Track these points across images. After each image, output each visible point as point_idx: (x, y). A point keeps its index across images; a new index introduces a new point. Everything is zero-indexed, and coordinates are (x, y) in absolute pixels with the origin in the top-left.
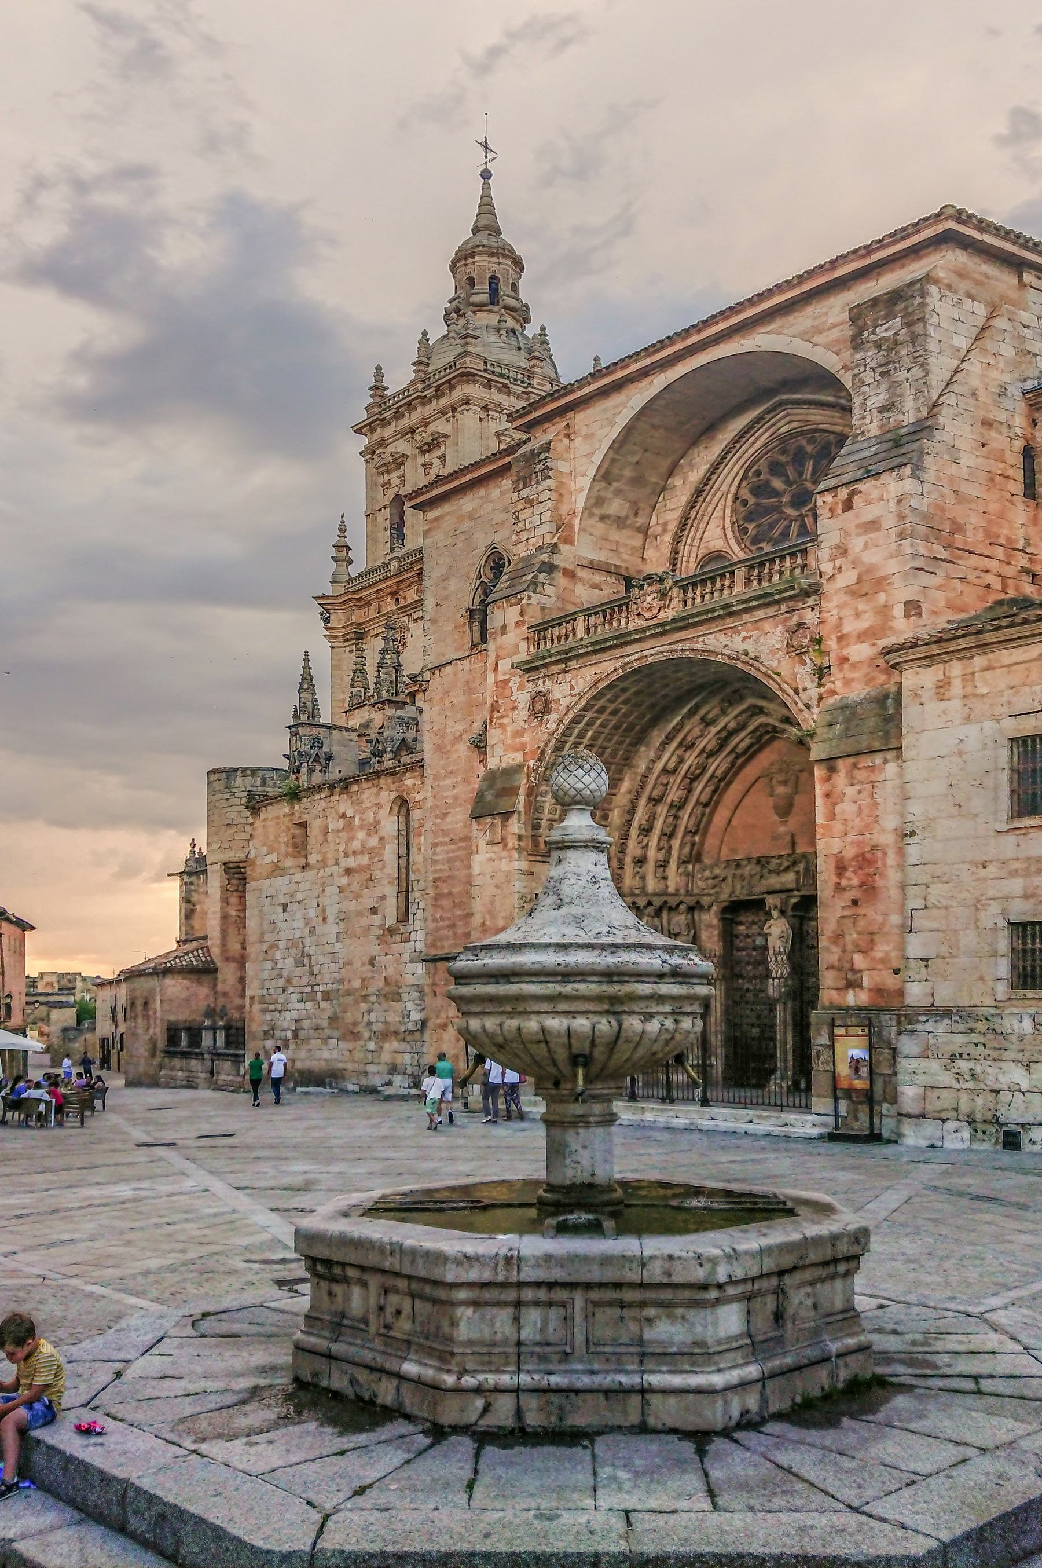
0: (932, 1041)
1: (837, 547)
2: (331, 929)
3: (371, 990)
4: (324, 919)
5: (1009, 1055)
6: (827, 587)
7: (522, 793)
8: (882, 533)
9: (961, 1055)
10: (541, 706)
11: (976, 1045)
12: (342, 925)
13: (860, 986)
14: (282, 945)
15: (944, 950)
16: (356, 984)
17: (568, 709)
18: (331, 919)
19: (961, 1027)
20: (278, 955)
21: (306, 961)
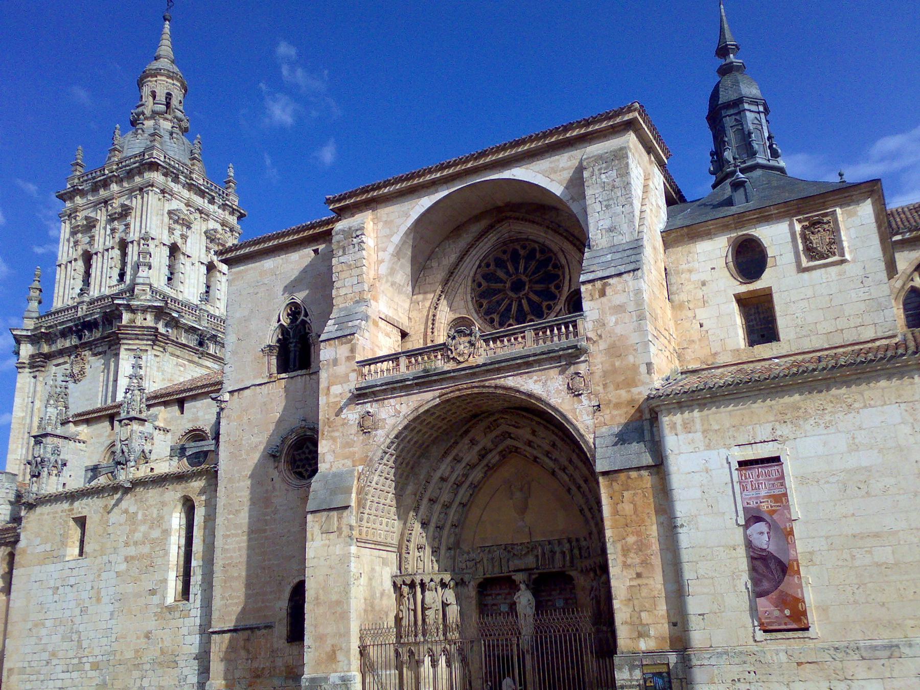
0: (716, 672)
1: (597, 321)
2: (106, 609)
3: (145, 659)
4: (99, 600)
5: (773, 678)
6: (592, 348)
7: (354, 490)
8: (627, 315)
9: (739, 680)
10: (365, 427)
11: (749, 673)
12: (117, 604)
13: (649, 636)
14: (48, 623)
15: (715, 607)
16: (129, 654)
17: (394, 427)
18: (105, 600)
19: (737, 660)
20: (43, 632)
21: (75, 637)
